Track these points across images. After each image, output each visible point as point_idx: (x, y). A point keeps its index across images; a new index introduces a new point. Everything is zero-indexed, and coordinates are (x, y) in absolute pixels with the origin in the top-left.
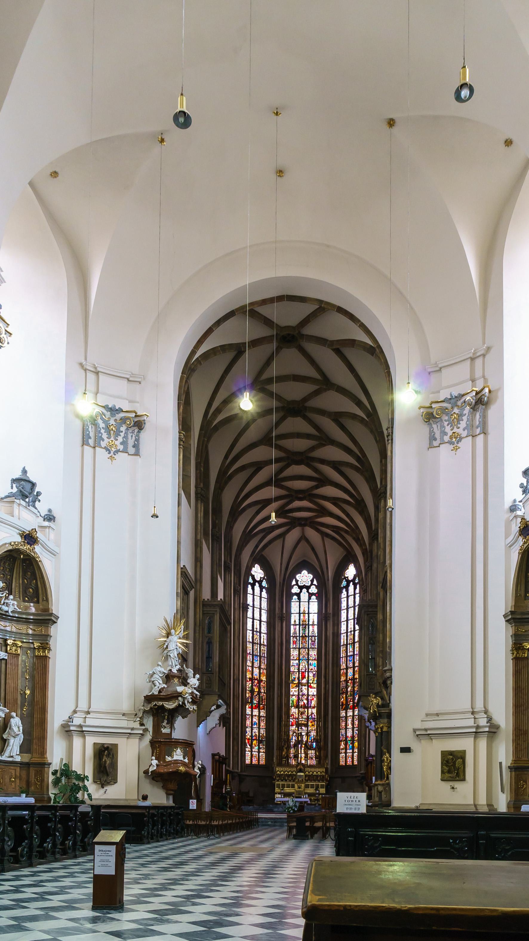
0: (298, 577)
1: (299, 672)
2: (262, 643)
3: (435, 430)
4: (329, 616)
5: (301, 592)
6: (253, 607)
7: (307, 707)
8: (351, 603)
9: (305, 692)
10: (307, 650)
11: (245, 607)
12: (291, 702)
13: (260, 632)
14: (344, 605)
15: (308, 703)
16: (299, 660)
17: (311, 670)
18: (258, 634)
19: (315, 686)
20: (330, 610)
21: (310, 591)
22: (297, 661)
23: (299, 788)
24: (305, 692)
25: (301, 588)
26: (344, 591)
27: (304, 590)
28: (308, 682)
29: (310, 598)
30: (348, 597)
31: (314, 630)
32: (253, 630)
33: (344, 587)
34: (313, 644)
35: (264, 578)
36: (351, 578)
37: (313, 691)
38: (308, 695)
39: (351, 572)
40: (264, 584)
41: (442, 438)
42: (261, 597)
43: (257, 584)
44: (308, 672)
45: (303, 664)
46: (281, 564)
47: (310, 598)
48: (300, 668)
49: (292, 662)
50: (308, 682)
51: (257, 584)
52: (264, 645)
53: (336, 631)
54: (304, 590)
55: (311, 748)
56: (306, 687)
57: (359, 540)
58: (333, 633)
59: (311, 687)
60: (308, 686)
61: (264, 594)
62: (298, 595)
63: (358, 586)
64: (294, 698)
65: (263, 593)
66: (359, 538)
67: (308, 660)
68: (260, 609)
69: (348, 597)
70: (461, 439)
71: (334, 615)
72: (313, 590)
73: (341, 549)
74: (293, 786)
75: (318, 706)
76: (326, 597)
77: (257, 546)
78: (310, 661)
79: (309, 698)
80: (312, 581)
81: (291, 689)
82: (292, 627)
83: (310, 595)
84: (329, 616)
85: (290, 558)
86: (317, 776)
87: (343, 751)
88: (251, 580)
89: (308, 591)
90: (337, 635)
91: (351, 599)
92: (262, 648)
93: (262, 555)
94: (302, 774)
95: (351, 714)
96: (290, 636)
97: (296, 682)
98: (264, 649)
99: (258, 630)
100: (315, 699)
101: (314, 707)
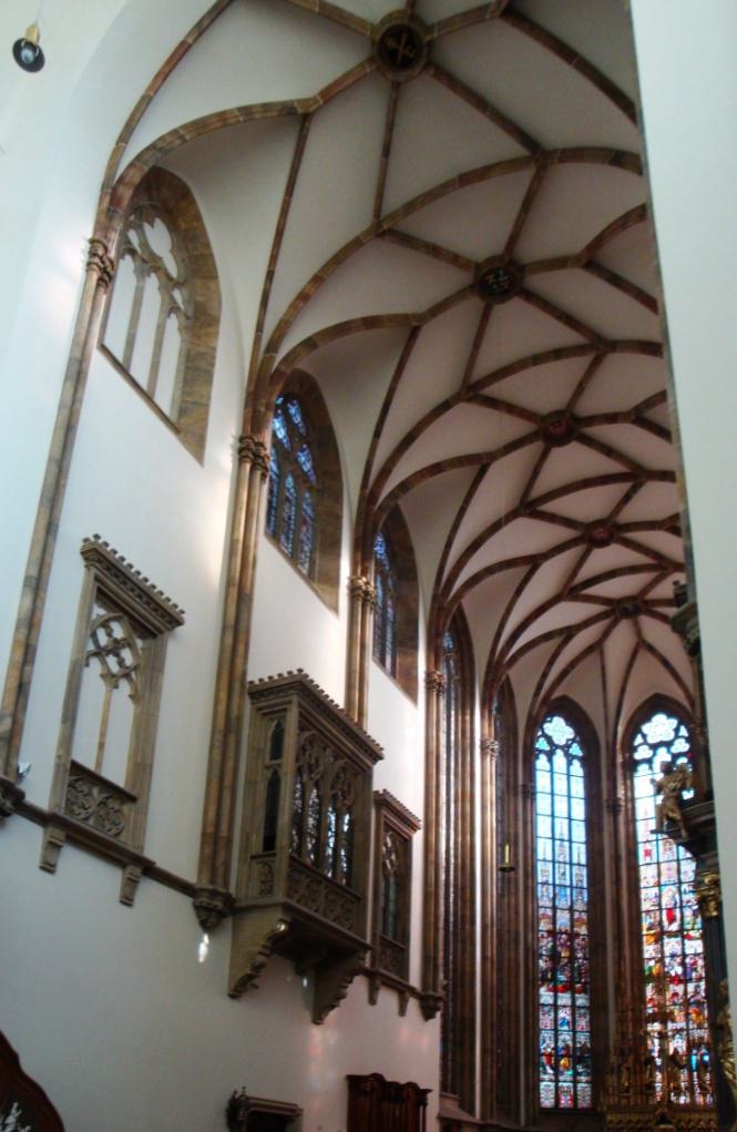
0: (646, 728)
2: (575, 860)
5: (655, 754)
10: (675, 864)
13: (570, 841)
15: (685, 972)
16: (659, 885)
17: (688, 902)
18: (567, 844)
22: (656, 890)
35: (573, 740)
38: (684, 956)
40: (576, 750)
42: (569, 775)
43: (559, 753)
44: (681, 907)
46: (605, 706)
51: (559, 753)
52: (579, 864)
56: (679, 939)
59: (690, 938)
60: (684, 937)
61: (576, 764)
62: (649, 761)
65: (572, 768)
67: (680, 883)
78: (684, 887)
79: (688, 960)
80: (677, 730)
85: (623, 690)
89: (669, 751)
96: (635, 843)
99: (566, 837)
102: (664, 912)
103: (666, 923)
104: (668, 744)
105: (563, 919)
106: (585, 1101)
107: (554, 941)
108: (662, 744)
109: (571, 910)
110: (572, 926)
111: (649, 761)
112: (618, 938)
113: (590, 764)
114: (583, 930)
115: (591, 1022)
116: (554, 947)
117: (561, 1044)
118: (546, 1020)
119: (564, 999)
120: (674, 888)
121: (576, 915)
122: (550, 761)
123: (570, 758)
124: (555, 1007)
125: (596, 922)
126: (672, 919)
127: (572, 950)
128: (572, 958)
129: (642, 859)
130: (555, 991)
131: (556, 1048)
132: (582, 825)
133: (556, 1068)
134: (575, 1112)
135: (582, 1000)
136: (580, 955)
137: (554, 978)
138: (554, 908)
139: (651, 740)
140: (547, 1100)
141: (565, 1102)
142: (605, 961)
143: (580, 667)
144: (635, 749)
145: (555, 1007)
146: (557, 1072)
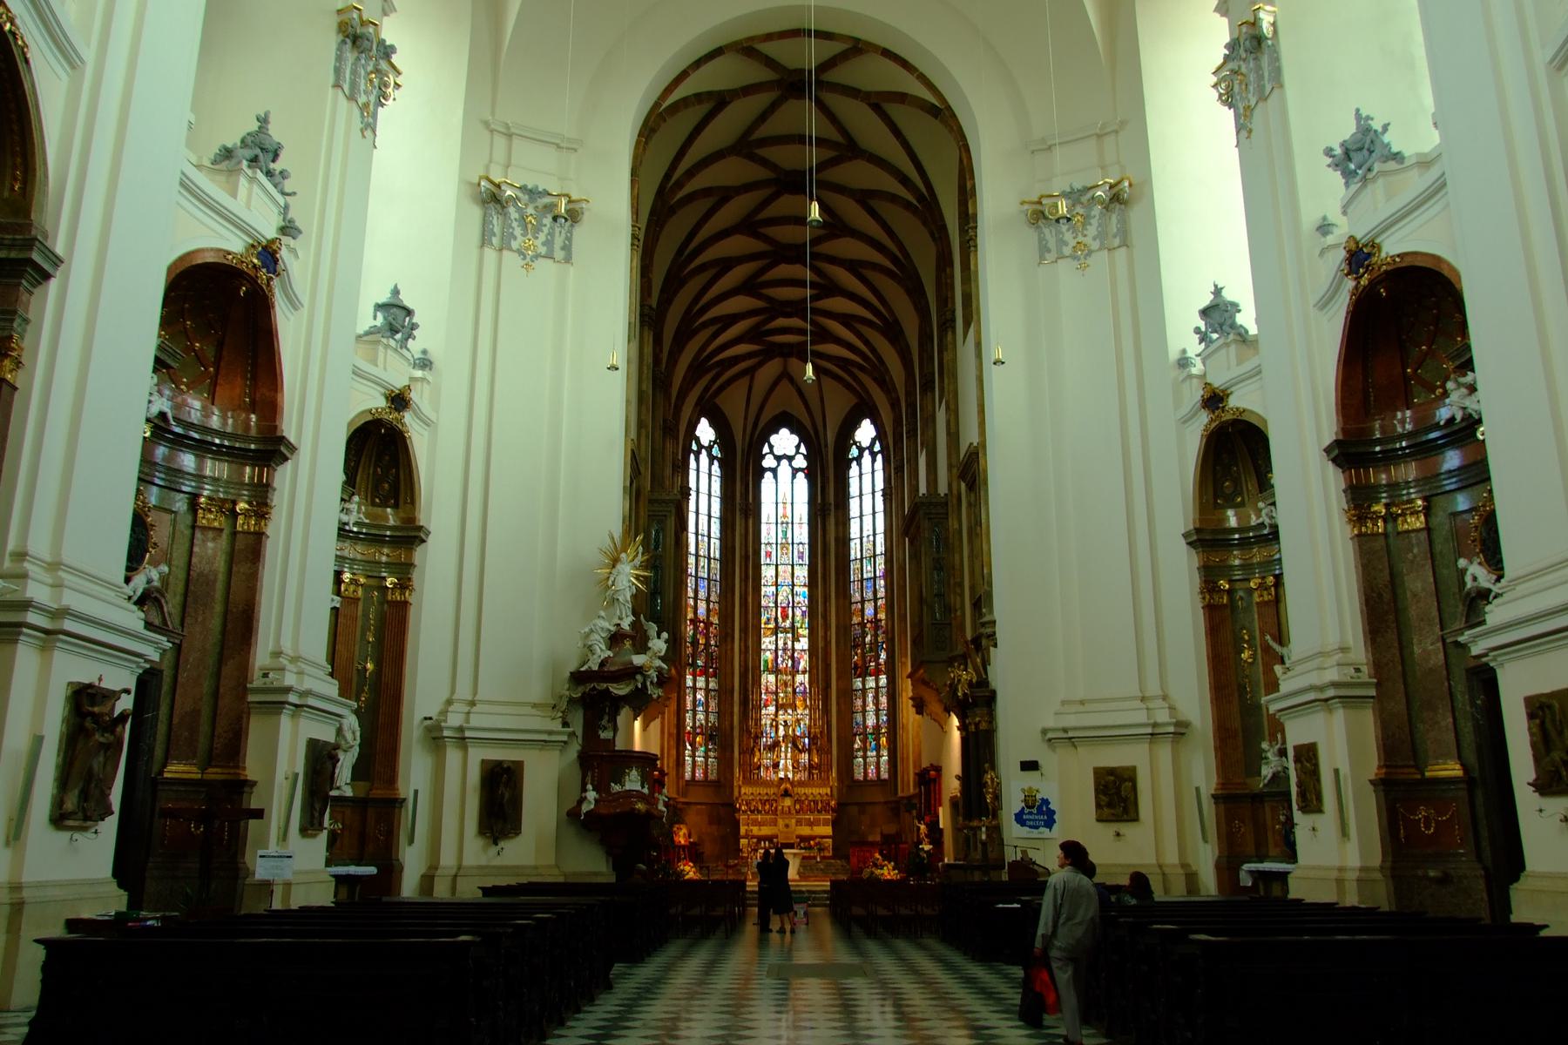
0: (774, 439)
4: (829, 506)
6: (698, 492)
7: (794, 671)
8: (867, 488)
9: (785, 647)
14: (854, 489)
16: (777, 585)
19: (806, 632)
24: (785, 647)
25: (778, 458)
26: (854, 464)
27: (784, 462)
29: (794, 476)
30: (861, 475)
31: (802, 534)
32: (697, 534)
34: (801, 557)
36: (866, 443)
37: (803, 644)
38: (793, 650)
39: (865, 432)
40: (716, 451)
42: (710, 475)
45: (784, 592)
46: (746, 418)
47: (794, 476)
49: (763, 589)
54: (784, 462)
57: (884, 383)
58: (837, 539)
61: (716, 467)
62: (774, 471)
63: (879, 457)
64: (768, 656)
68: (710, 495)
69: (861, 475)
71: (837, 507)
72: (800, 462)
74: (775, 823)
75: (812, 671)
77: (707, 389)
80: (798, 447)
82: (764, 527)
83: (795, 471)
84: (829, 506)
86: (816, 802)
88: (694, 447)
90: (844, 541)
91: (867, 479)
97: (772, 626)
98: (716, 565)
100: (806, 657)
104: (790, 459)
105: (702, 606)
107: (696, 629)
109: (708, 601)
112: (744, 630)
114: (715, 620)
115: (719, 705)
118: (689, 699)
119: (701, 682)
120: (788, 590)
123: (712, 458)
124: (695, 689)
126: (785, 617)
127: (707, 639)
128: (707, 645)
131: (694, 727)
134: (706, 782)
135: (712, 685)
137: (694, 665)
138: (696, 598)
139: (777, 452)
140: (688, 776)
142: (732, 649)
144: (763, 457)
146: (694, 750)
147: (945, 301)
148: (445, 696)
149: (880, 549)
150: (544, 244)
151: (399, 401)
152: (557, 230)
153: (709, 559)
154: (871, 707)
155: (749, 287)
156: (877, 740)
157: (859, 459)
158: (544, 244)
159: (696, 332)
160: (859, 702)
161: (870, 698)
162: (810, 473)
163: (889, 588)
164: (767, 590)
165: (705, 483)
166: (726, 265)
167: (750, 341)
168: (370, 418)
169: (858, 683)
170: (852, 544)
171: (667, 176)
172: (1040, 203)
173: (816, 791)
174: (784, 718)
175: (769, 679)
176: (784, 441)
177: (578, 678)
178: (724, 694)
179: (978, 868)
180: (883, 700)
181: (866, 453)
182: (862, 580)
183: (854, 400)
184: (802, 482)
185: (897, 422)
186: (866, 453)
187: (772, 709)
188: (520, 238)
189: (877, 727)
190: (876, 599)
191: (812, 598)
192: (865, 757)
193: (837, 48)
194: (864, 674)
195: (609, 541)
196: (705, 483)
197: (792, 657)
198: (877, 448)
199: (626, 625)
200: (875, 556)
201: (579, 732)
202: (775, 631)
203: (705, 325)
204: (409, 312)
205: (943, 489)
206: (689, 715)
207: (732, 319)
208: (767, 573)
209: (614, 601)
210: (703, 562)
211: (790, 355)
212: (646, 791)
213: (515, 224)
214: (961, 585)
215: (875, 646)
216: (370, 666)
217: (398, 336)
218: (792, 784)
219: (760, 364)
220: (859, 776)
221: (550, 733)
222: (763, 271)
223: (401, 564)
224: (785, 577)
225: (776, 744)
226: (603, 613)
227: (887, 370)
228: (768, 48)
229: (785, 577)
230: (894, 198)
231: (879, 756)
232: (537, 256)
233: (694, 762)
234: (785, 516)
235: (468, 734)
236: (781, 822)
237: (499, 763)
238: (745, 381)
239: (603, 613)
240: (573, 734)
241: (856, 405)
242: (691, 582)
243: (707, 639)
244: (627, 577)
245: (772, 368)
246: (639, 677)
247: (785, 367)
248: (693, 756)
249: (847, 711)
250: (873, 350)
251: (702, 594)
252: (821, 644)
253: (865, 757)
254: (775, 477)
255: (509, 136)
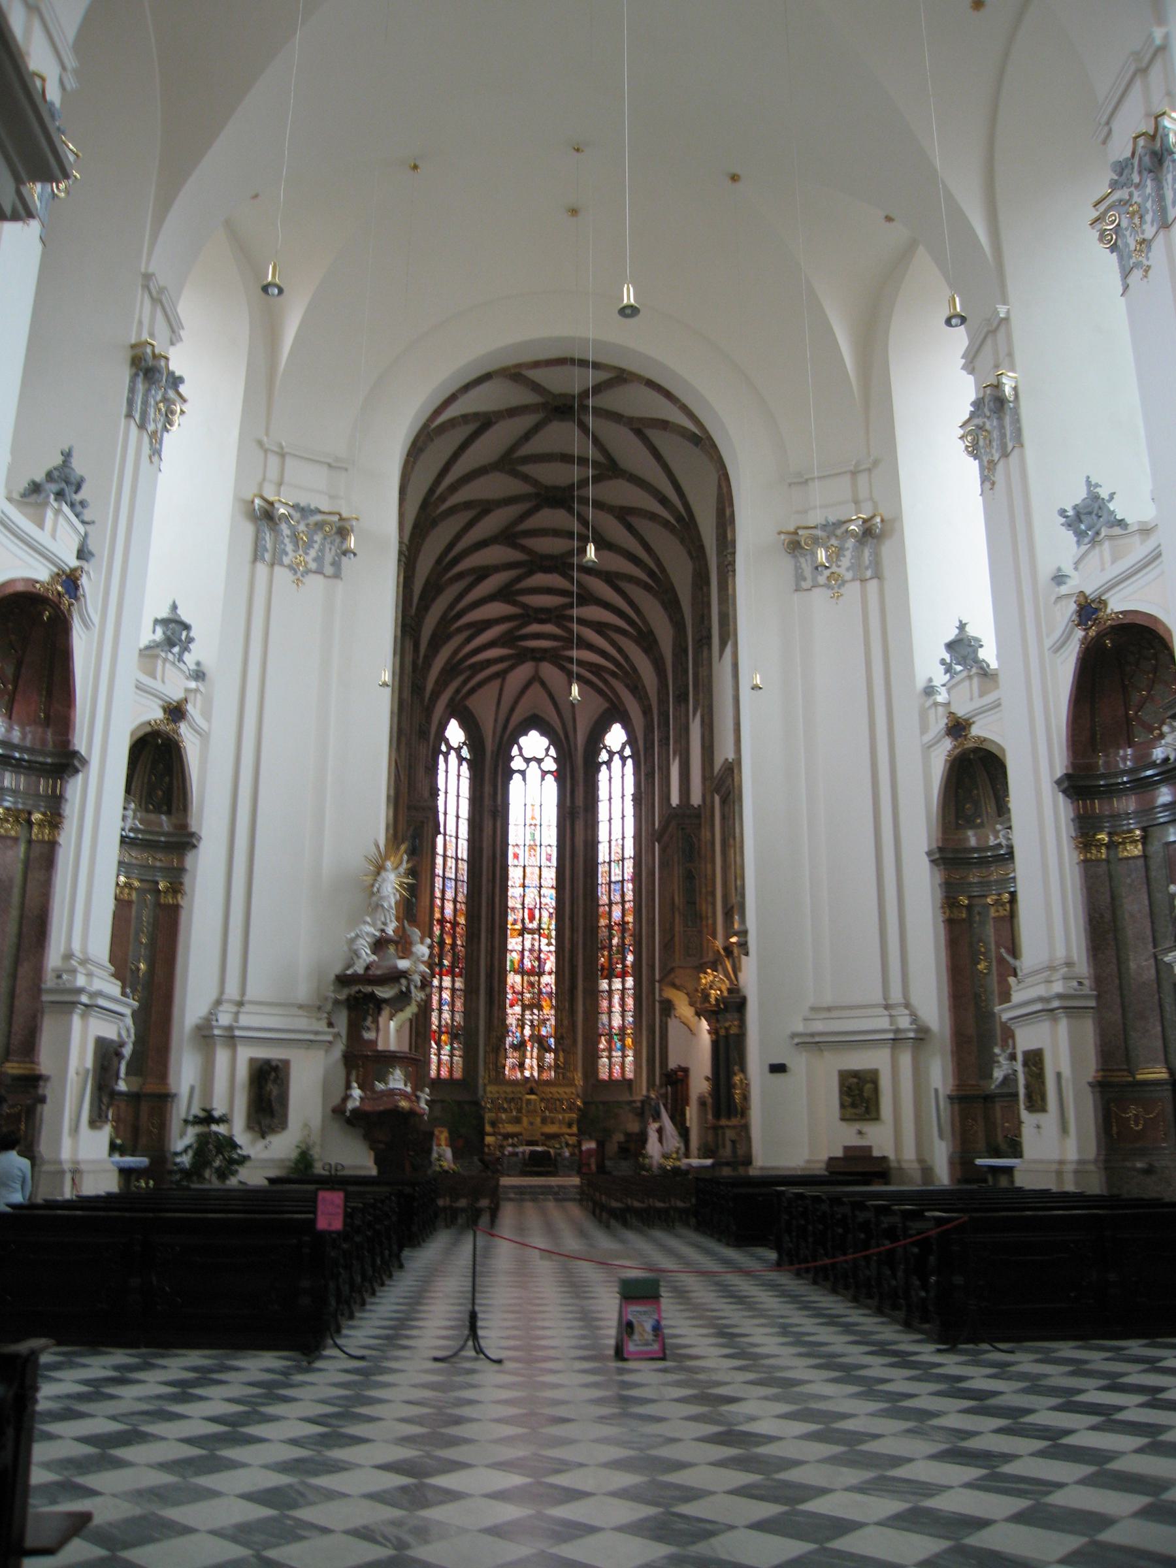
0: (523, 740)
1: (523, 908)
3: (804, 565)
7: (540, 974)
9: (531, 946)
10: (537, 869)
11: (434, 792)
12: (508, 963)
13: (457, 838)
14: (603, 793)
15: (539, 966)
16: (524, 886)
18: (454, 840)
20: (580, 802)
21: (543, 765)
23: (531, 1124)
24: (531, 946)
25: (527, 761)
26: (604, 768)
27: (533, 764)
28: (540, 928)
29: (543, 779)
33: (604, 763)
34: (549, 860)
35: (464, 743)
36: (616, 748)
38: (540, 951)
39: (616, 736)
40: (465, 752)
41: (814, 579)
43: (453, 753)
46: (496, 720)
47: (543, 779)
48: (526, 902)
50: (540, 928)
51: (453, 753)
53: (590, 838)
54: (533, 764)
55: (549, 1050)
57: (637, 689)
58: (586, 842)
62: (523, 773)
63: (629, 762)
64: (515, 956)
66: (636, 687)
67: (541, 887)
70: (844, 582)
71: (586, 810)
72: (550, 765)
73: (600, 700)
74: (517, 1121)
75: (559, 973)
76: (573, 778)
77: (458, 691)
78: (543, 891)
80: (547, 750)
81: (510, 940)
82: (512, 829)
83: (544, 773)
87: (605, 1054)
88: (444, 748)
92: (460, 866)
93: (466, 708)
94: (533, 1097)
95: (619, 986)
96: (507, 844)
97: (518, 926)
98: (463, 866)
100: (553, 958)
101: (550, 974)
102: (526, 911)
103: (527, 921)
104: (539, 761)
105: (449, 907)
106: (458, 1074)
108: (535, 759)
109: (455, 901)
110: (455, 916)
111: (523, 773)
112: (491, 931)
113: (476, 767)
114: (462, 920)
115: (465, 1005)
116: (441, 935)
117: (443, 1023)
119: (447, 982)
121: (458, 906)
122: (446, 761)
123: (461, 759)
124: (441, 988)
125: (473, 914)
127: (454, 938)
128: (454, 945)
129: (511, 860)
130: (441, 975)
131: (439, 1026)
132: (466, 823)
133: (438, 1043)
134: (451, 1081)
135: (459, 984)
136: (459, 942)
138: (443, 899)
139: (528, 755)
140: (433, 1074)
141: (444, 1073)
142: (479, 950)
143: (486, 687)
144: (512, 758)
145: (441, 988)
146: (440, 1048)
147: (703, 618)
148: (213, 995)
149: (629, 851)
150: (315, 560)
151: (176, 712)
152: (327, 546)
153: (457, 859)
154: (617, 1008)
155: (504, 594)
156: (622, 1040)
157: (608, 763)
158: (315, 560)
159: (449, 637)
160: (605, 1004)
161: (616, 999)
162: (559, 776)
163: (637, 891)
164: (514, 892)
165: (454, 784)
166: (482, 574)
167: (503, 646)
168: (148, 729)
169: (604, 985)
170: (601, 847)
171: (432, 491)
172: (796, 533)
173: (561, 1090)
174: (527, 1019)
175: (514, 979)
176: (534, 743)
177: (343, 980)
178: (470, 992)
179: (728, 1164)
180: (630, 1002)
181: (616, 757)
182: (610, 883)
183: (606, 705)
184: (551, 784)
185: (649, 729)
186: (616, 757)
187: (518, 1009)
188: (291, 554)
189: (623, 1028)
190: (623, 902)
191: (559, 900)
192: (610, 1057)
193: (603, 376)
194: (610, 977)
195: (374, 849)
196: (454, 784)
197: (539, 959)
198: (628, 752)
199: (390, 931)
200: (623, 859)
201: (344, 1032)
202: (522, 933)
203: (459, 630)
204: (187, 627)
205: (696, 799)
206: (435, 1014)
207: (487, 624)
208: (515, 875)
209: (378, 906)
210: (451, 863)
211: (541, 659)
212: (409, 1089)
213: (287, 541)
214: (713, 894)
215: (622, 949)
216: (142, 966)
217: (176, 650)
218: (539, 1082)
219: (512, 668)
220: (604, 1075)
221: (317, 1033)
222: (519, 579)
223: (174, 868)
224: (532, 880)
225: (520, 1046)
226: (368, 919)
227: (639, 677)
228: (535, 375)
229: (532, 880)
230: (653, 517)
231: (624, 1056)
232: (308, 572)
233: (439, 1060)
234: (533, 818)
235: (237, 1033)
236: (525, 1120)
237: (268, 1062)
238: (496, 684)
239: (368, 919)
240: (337, 1035)
241: (606, 711)
242: (438, 883)
243: (454, 938)
244: (391, 885)
245: (523, 672)
246: (404, 981)
247: (537, 671)
248: (439, 1055)
249: (593, 1012)
250: (626, 658)
251: (450, 894)
252: (567, 945)
253: (610, 1057)
254: (524, 779)
255: (283, 456)
